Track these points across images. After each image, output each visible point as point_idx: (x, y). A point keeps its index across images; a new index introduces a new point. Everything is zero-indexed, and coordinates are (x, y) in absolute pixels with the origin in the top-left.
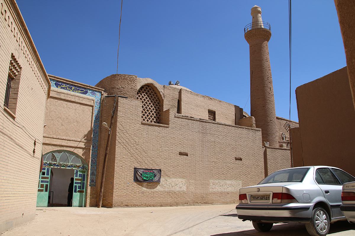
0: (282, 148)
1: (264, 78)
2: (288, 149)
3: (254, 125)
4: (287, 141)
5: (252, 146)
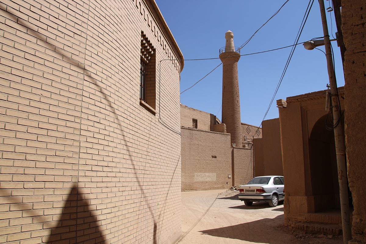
0: (245, 148)
1: (233, 93)
2: (249, 148)
3: (225, 130)
4: (248, 142)
5: (224, 147)
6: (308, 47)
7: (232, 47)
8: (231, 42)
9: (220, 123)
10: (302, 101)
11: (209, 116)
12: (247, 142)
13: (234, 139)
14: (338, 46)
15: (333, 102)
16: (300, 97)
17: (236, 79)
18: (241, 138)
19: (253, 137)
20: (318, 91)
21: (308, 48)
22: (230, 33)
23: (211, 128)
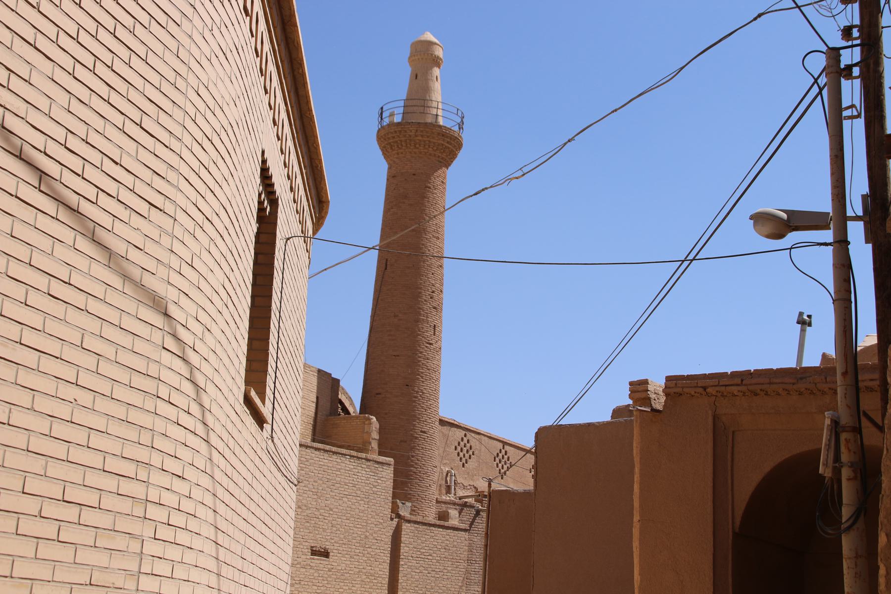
0: (446, 524)
1: (420, 293)
2: (463, 526)
3: (375, 445)
4: (460, 498)
5: (363, 512)
6: (768, 228)
7: (434, 104)
8: (431, 84)
9: (351, 410)
10: (719, 394)
11: (314, 380)
12: (457, 501)
13: (404, 484)
14: (867, 242)
15: (843, 449)
16: (715, 382)
17: (438, 238)
18: (436, 479)
19: (490, 482)
20: (779, 367)
21: (766, 233)
22: (430, 43)
23: (318, 428)
